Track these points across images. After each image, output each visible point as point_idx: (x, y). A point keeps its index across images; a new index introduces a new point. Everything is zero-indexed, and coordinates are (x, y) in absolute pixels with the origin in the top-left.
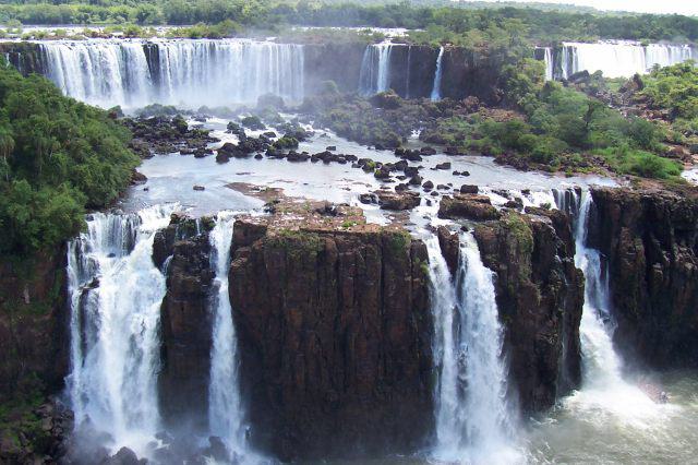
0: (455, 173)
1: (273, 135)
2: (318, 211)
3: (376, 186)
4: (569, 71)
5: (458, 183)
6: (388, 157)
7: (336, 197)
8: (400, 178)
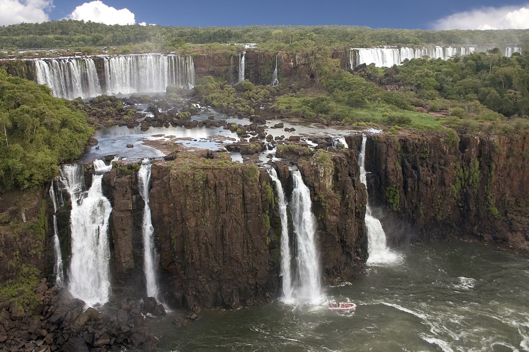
2: (202, 156)
4: (355, 63)
6: (246, 122)
7: (213, 147)
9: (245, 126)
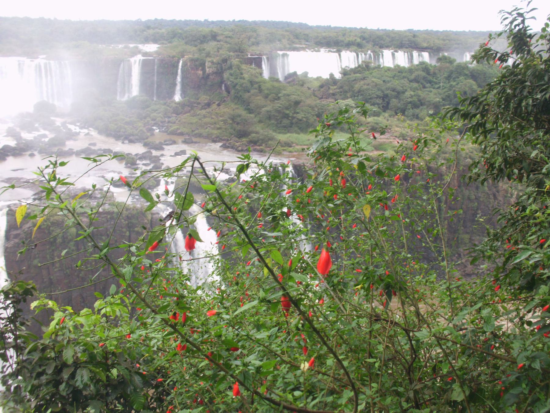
1: (45, 136)
6: (137, 149)
9: (136, 155)
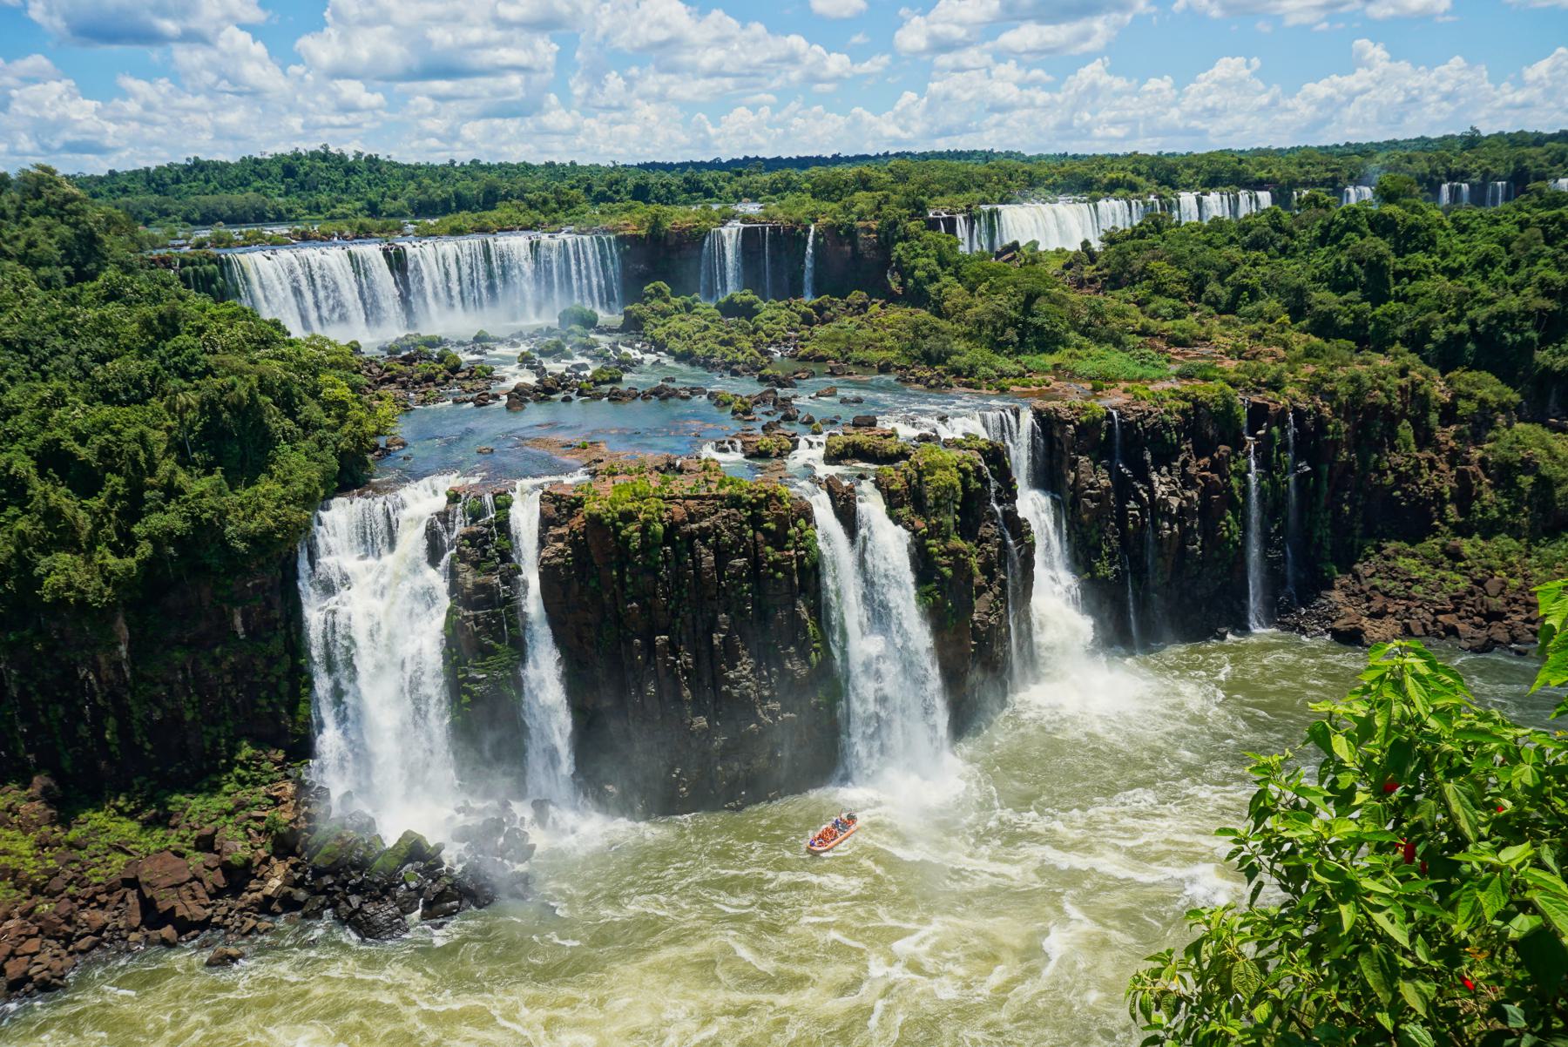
0: (844, 401)
1: (585, 367)
3: (734, 426)
5: (849, 414)
6: (748, 387)
8: (767, 414)
